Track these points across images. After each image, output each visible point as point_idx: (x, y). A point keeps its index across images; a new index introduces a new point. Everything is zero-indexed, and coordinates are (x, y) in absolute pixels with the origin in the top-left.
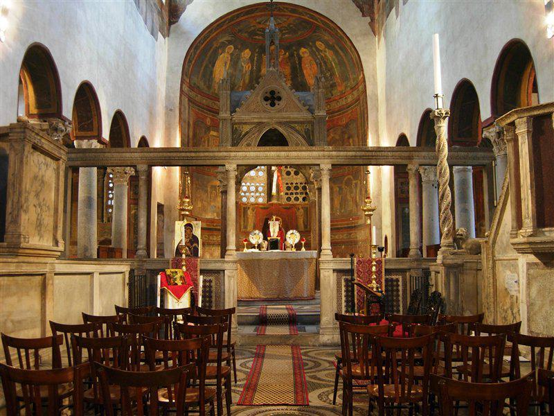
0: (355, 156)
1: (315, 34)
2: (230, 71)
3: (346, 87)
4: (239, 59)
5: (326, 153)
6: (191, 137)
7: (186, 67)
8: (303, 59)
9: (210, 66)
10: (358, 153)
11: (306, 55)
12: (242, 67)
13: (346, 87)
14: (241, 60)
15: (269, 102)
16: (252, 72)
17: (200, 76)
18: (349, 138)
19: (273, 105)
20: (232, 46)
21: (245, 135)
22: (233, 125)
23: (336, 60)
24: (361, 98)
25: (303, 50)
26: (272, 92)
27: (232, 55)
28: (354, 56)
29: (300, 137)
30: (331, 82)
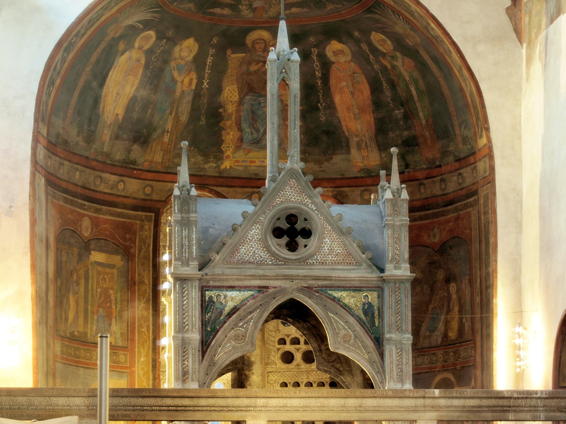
0: (480, 407)
1: (369, 15)
2: (143, 93)
3: (445, 153)
4: (166, 62)
5: (428, 402)
6: (51, 275)
7: (44, 98)
8: (334, 68)
9: (95, 84)
10: (485, 402)
11: (342, 59)
12: (174, 81)
13: (445, 153)
14: (173, 64)
15: (285, 239)
16: (197, 95)
17: (71, 111)
18: (448, 280)
19: (292, 247)
20: (152, 33)
21: (230, 315)
22: (203, 290)
23: (421, 83)
24: (482, 193)
25: (335, 46)
26: (292, 218)
27: (149, 52)
28: (469, 87)
29: (351, 320)
30: (406, 133)
